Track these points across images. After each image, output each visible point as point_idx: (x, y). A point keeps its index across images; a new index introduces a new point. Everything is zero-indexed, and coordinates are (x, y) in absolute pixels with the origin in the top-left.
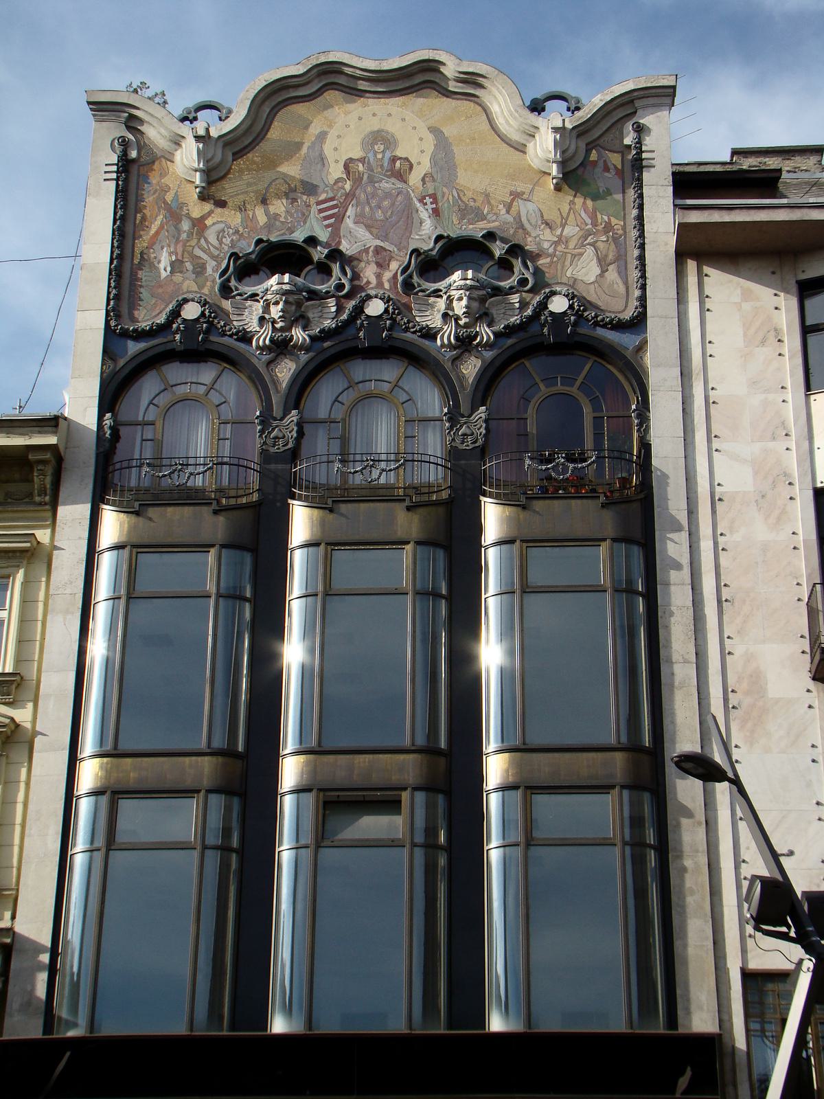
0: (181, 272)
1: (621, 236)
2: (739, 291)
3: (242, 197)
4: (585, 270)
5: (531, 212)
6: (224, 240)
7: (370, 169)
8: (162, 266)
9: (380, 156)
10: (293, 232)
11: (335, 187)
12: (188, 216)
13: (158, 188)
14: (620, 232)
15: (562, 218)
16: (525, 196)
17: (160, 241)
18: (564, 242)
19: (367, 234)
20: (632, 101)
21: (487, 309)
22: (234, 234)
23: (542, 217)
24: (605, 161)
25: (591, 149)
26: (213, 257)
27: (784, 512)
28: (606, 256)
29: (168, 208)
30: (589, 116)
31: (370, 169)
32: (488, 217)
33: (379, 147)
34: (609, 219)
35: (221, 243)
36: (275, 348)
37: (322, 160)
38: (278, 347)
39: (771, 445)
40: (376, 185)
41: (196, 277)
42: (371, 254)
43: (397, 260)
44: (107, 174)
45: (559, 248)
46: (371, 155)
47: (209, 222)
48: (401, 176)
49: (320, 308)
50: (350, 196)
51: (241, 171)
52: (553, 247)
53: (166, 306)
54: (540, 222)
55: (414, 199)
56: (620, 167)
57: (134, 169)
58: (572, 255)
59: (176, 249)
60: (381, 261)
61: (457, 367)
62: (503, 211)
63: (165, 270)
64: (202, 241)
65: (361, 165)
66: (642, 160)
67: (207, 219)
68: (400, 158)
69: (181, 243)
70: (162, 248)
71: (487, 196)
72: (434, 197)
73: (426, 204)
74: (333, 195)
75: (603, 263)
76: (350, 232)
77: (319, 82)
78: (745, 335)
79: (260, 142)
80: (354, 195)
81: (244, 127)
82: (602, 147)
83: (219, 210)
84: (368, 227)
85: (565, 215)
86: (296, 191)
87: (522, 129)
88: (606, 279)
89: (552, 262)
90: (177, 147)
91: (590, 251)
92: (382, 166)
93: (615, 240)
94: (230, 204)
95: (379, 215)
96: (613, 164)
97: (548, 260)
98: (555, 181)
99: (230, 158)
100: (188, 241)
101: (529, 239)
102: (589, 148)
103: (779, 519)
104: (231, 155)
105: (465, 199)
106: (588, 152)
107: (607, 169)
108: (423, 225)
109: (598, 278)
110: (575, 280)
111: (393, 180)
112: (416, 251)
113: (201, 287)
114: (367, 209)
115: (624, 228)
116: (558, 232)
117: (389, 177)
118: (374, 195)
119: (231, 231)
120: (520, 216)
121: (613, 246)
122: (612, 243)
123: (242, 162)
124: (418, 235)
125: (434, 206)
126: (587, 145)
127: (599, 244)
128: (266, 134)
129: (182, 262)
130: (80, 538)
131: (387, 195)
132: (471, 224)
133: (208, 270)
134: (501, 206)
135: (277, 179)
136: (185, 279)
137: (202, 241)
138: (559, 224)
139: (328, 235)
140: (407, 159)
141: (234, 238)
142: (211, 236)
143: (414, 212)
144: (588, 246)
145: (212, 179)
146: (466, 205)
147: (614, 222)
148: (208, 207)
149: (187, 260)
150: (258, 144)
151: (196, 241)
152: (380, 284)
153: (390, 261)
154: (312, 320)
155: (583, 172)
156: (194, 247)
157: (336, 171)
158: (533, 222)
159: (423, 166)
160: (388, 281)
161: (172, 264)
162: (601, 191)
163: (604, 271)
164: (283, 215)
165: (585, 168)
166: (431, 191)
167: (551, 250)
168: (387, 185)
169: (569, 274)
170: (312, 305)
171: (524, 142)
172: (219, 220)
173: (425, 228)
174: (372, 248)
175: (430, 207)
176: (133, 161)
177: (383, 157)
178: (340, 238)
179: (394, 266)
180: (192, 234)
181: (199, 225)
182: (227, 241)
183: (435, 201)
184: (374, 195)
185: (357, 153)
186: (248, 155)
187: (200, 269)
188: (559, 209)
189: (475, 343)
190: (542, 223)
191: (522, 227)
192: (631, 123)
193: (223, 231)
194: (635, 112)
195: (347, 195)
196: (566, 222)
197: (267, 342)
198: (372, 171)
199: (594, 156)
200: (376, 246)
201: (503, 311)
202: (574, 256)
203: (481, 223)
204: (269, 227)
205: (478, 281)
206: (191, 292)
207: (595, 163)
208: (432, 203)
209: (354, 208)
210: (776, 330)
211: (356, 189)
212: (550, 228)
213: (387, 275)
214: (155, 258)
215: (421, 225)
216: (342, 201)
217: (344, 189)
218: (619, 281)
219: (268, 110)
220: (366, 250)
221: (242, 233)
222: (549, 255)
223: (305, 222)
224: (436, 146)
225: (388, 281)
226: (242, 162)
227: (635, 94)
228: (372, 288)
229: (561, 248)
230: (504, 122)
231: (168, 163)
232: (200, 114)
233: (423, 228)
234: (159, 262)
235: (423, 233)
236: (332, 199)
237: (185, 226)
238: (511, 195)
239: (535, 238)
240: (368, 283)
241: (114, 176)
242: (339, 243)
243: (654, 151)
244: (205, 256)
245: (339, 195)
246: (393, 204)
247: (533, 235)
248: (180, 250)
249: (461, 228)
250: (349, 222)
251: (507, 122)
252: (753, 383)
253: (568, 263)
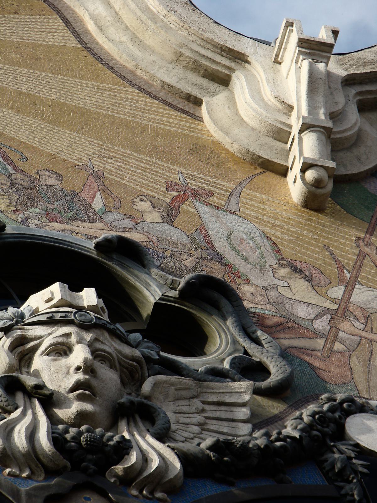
15: (341, 268)
23: (278, 251)
54: (272, 261)
62: (154, 216)
87: (189, 53)
98: (310, 175)
158: (254, 257)
171: (195, 92)
188: (327, 247)
189: (119, 469)
201: (197, 418)
230: (124, 39)
249: (24, 222)
251: (135, 39)
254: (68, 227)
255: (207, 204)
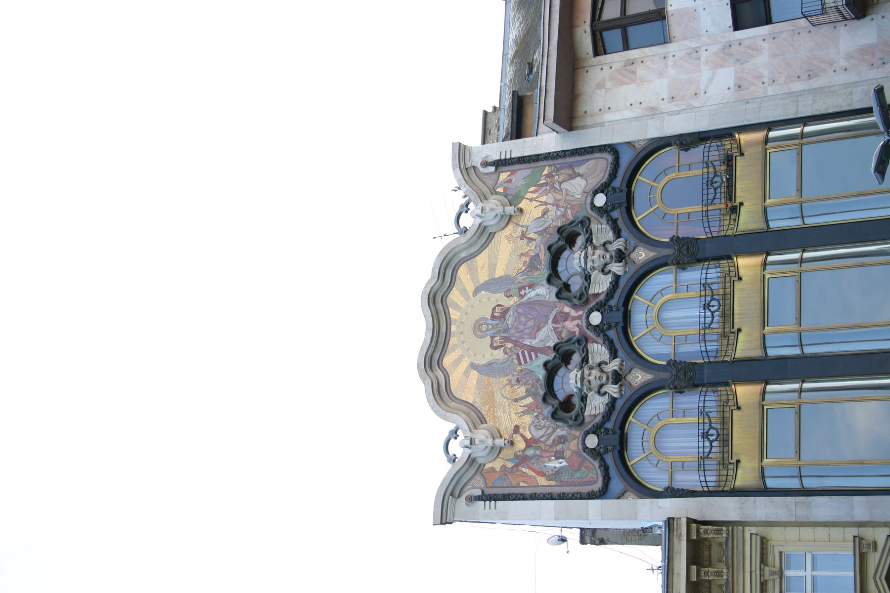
0: (563, 452)
1: (556, 167)
2: (598, 91)
3: (513, 415)
4: (577, 187)
5: (535, 226)
6: (542, 425)
7: (498, 332)
8: (558, 465)
9: (490, 327)
10: (539, 379)
11: (510, 354)
12: (523, 451)
13: (502, 473)
14: (553, 168)
15: (540, 205)
16: (525, 230)
17: (540, 468)
18: (557, 202)
19: (544, 329)
20: (466, 169)
21: (601, 245)
22: (538, 419)
24: (504, 183)
25: (496, 192)
26: (554, 431)
27: (749, 47)
28: (569, 175)
29: (517, 466)
30: (475, 193)
31: (498, 332)
32: (537, 252)
33: (484, 327)
34: (544, 175)
35: (544, 427)
36: (621, 382)
37: (489, 364)
38: (620, 381)
39: (703, 59)
40: (510, 327)
41: (567, 441)
42: (558, 326)
43: (563, 308)
44: (491, 507)
45: (561, 205)
46: (488, 333)
47: (529, 436)
48: (505, 311)
49: (594, 354)
50: (516, 343)
51: (495, 418)
52: (560, 209)
53: (588, 459)
54: (543, 219)
55: (522, 301)
56: (509, 173)
57: (488, 491)
58: (566, 196)
59: (546, 457)
60: (563, 319)
61: (639, 261)
62: (534, 243)
63: (561, 463)
64: (542, 439)
65: (495, 339)
66: (505, 160)
67: (526, 438)
68: (493, 313)
69: (544, 455)
70: (546, 466)
71: (522, 254)
72: (520, 289)
73: (525, 293)
74: (515, 355)
75: (572, 177)
76: (542, 341)
77: (436, 370)
78: (627, 84)
79: (475, 407)
80: (516, 341)
81: (464, 416)
82: (494, 187)
83: (521, 430)
84: (539, 330)
85: (540, 203)
86: (510, 380)
88: (584, 173)
89: (571, 208)
90: (475, 462)
91: (565, 185)
92: (497, 324)
93: (558, 170)
94: (517, 423)
95: (531, 323)
96: (508, 176)
97: (569, 211)
99: (484, 425)
100: (542, 449)
101: (554, 224)
102: (494, 192)
103: (754, 49)
104: (482, 425)
105: (523, 268)
106: (497, 193)
107: (510, 181)
108: (539, 293)
109: (583, 178)
110: (584, 192)
111: (507, 316)
112: (558, 295)
113: (575, 437)
114: (526, 331)
115: (550, 166)
116: (549, 207)
117: (505, 320)
118: (516, 328)
119: (536, 421)
120: (539, 231)
121: (562, 171)
122: (560, 172)
123: (488, 418)
124: (546, 295)
125: (527, 288)
126: (492, 195)
127: (561, 179)
128: (469, 403)
129: (556, 452)
130: (754, 502)
131: (517, 319)
132: (541, 263)
133: (563, 434)
134: (530, 244)
135: (501, 393)
136: (569, 448)
137: (542, 439)
138: (544, 207)
139: (543, 355)
140: (494, 309)
141: (541, 418)
142: (538, 434)
143: (531, 300)
144: (561, 186)
145: (499, 436)
146: (528, 267)
147: (546, 172)
148: (518, 438)
149: (555, 449)
150: (476, 408)
151: (542, 444)
152: (579, 317)
153: (563, 313)
154: (602, 360)
155: (511, 195)
156: (546, 445)
157: (499, 354)
158: (543, 223)
159: (501, 299)
160: (577, 312)
161: (557, 458)
162: (524, 183)
163: (579, 175)
164: (527, 386)
165: (508, 194)
166: (517, 291)
167: (562, 210)
168: (510, 320)
169: (579, 197)
170: (592, 359)
171: (488, 233)
172: (528, 429)
173: (542, 292)
174: (554, 326)
175: (527, 290)
176: (483, 492)
177: (490, 324)
178: (545, 347)
179: (567, 309)
180: (536, 447)
181: (529, 443)
182: (543, 423)
183: (524, 288)
184: (516, 328)
185: (488, 340)
186: (483, 414)
187: (562, 440)
188: (535, 208)
190: (544, 217)
191: (545, 230)
192: (481, 169)
193: (535, 426)
194: (474, 167)
195: (516, 346)
196: (545, 202)
197: (616, 386)
198: (500, 330)
199: (500, 190)
200: (553, 322)
202: (567, 194)
203: (540, 256)
204: (534, 395)
205: (582, 252)
206: (578, 444)
207: (505, 189)
208: (525, 289)
209: (525, 340)
210: (625, 66)
211: (512, 340)
212: (547, 212)
213: (573, 313)
214: (552, 470)
215: (539, 295)
216: (520, 348)
217: (512, 347)
218: (587, 164)
219: (453, 403)
220: (555, 329)
221: (538, 413)
222: (566, 211)
223: (534, 372)
224: (486, 291)
225: (577, 312)
226: (488, 418)
227: (462, 166)
228: (582, 323)
229: (561, 204)
231: (485, 468)
232: (451, 453)
233: (542, 293)
234: (555, 467)
235: (545, 293)
236: (518, 355)
237: (530, 452)
238: (523, 239)
239: (553, 221)
240: (578, 325)
241: (493, 502)
242: (549, 347)
243: (501, 152)
244: (552, 438)
245: (515, 351)
246: (524, 315)
247: (551, 223)
248: (548, 454)
249: (544, 269)
250: (535, 343)
252: (661, 75)
253: (572, 198)
254: (543, 260)
255: (526, 232)
